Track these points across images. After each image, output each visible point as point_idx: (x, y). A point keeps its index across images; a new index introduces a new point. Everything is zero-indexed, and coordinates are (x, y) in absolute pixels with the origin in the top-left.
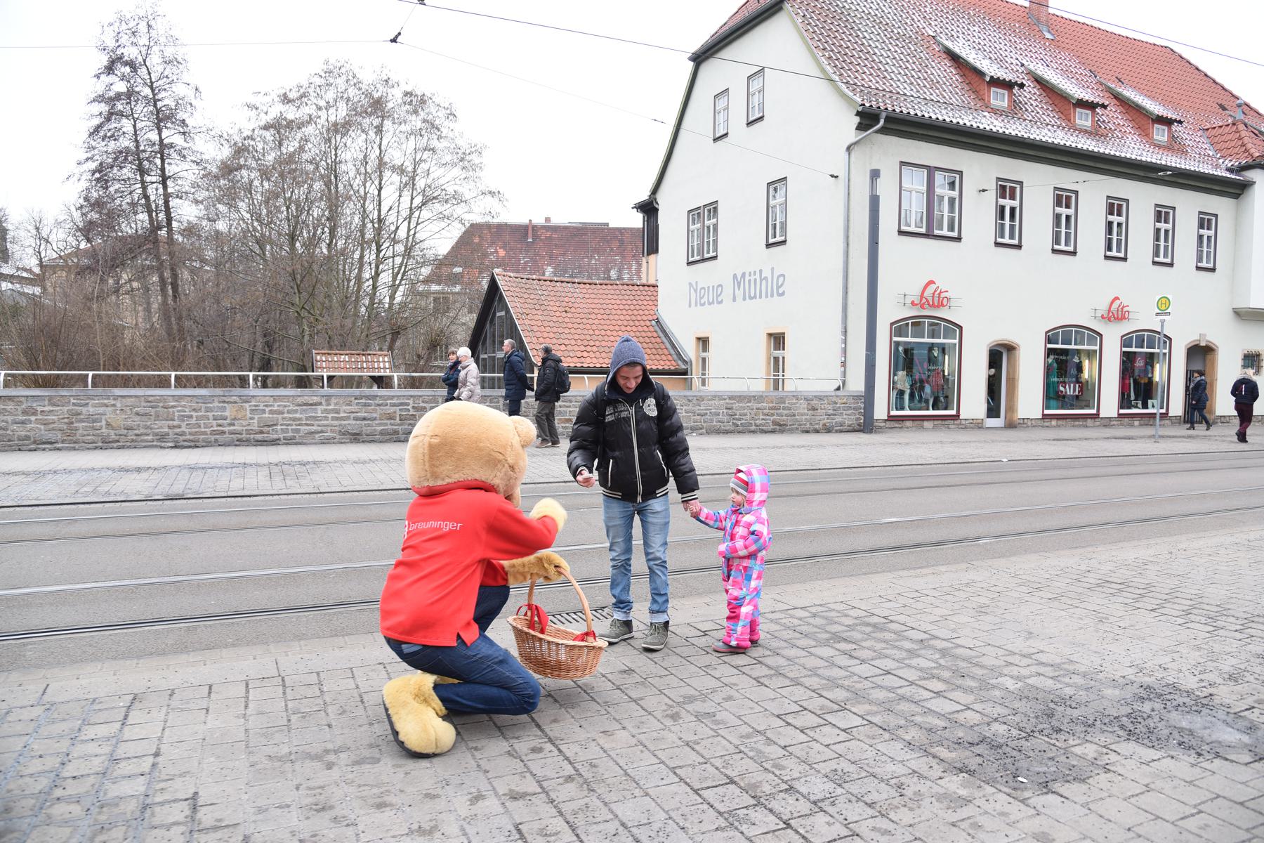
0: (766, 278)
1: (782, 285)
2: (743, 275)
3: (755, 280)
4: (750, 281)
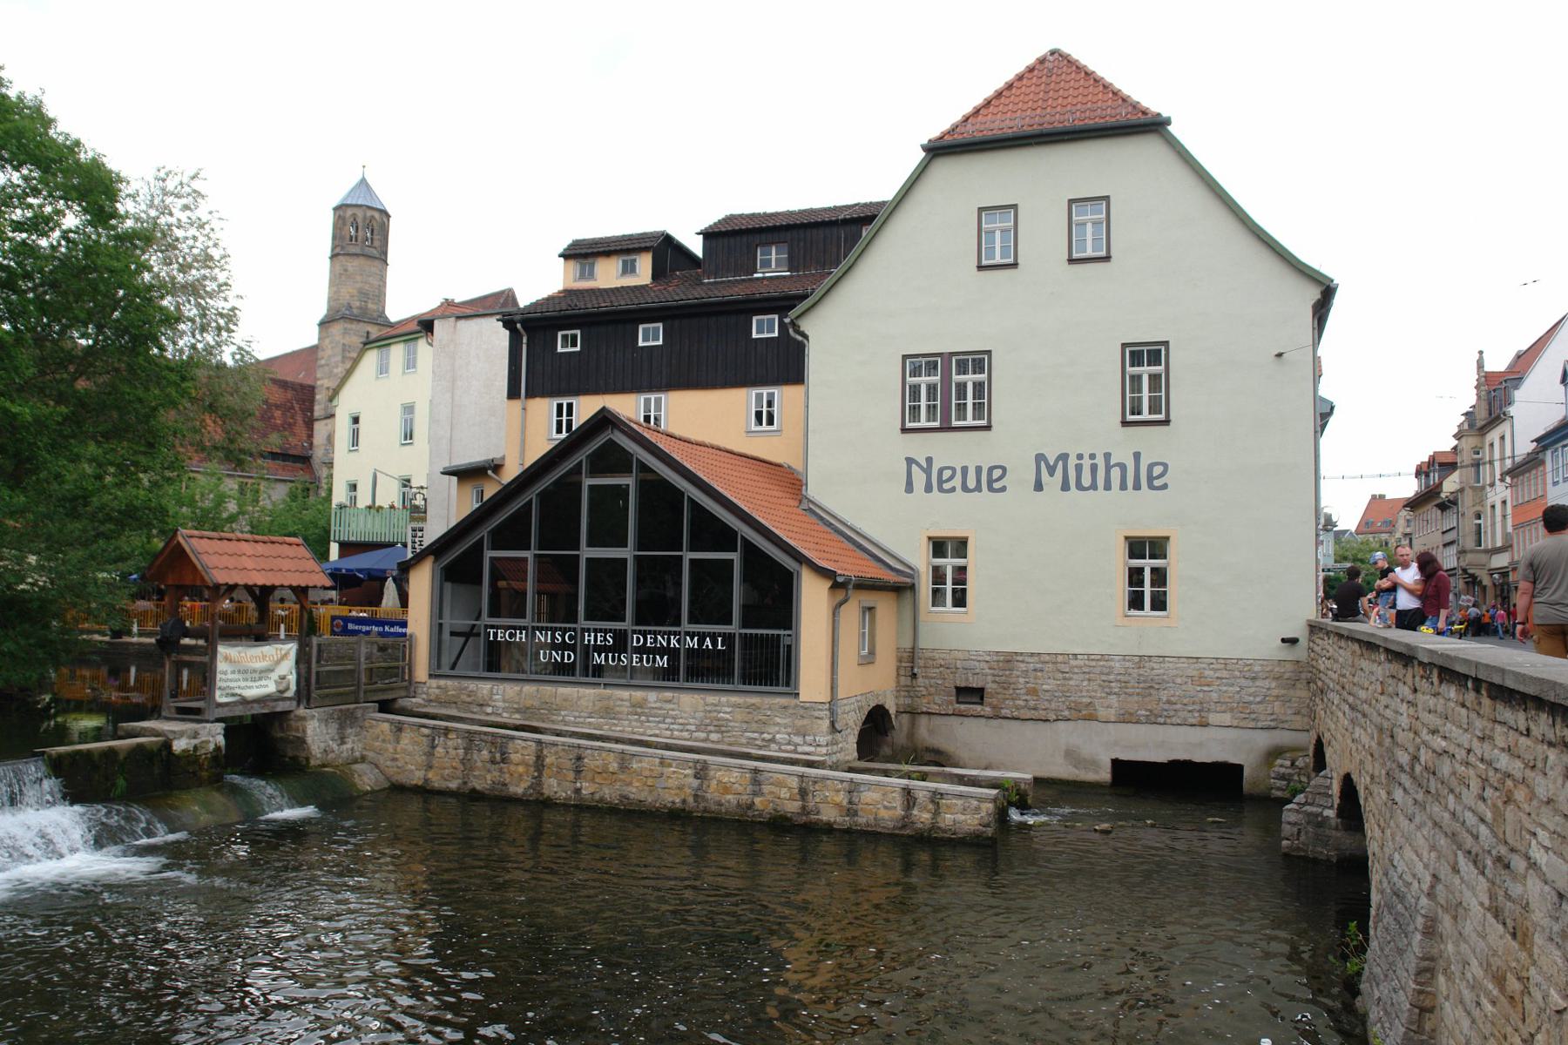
2: (1064, 457)
3: (1094, 468)
4: (1079, 468)
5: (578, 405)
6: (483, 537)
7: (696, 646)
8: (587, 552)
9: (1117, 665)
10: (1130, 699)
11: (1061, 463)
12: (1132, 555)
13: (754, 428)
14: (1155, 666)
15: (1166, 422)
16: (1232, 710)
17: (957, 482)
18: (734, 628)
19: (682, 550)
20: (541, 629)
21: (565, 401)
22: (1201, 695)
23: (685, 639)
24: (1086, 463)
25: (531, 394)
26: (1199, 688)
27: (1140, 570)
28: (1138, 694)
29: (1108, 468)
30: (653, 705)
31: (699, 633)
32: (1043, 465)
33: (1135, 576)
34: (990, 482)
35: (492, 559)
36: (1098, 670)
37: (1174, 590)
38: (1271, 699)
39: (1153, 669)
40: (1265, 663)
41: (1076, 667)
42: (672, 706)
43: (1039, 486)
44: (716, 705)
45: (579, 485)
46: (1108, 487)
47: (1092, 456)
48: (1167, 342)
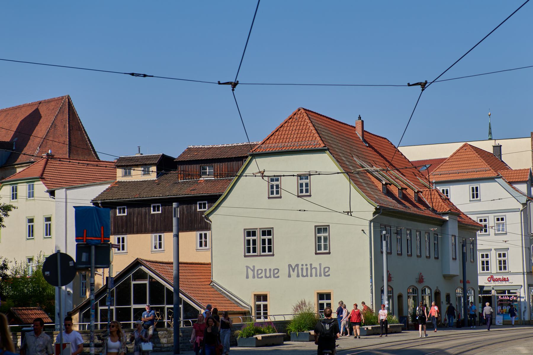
0: (316, 268)
1: (327, 272)
2: (297, 265)
3: (307, 269)
4: (302, 269)
8: (134, 306)
11: (296, 267)
13: (199, 248)
15: (329, 253)
17: (263, 274)
19: (164, 305)
21: (121, 237)
24: (304, 267)
27: (323, 304)
29: (311, 269)
32: (291, 268)
34: (274, 274)
35: (101, 310)
43: (290, 276)
45: (130, 284)
46: (311, 276)
47: (306, 265)
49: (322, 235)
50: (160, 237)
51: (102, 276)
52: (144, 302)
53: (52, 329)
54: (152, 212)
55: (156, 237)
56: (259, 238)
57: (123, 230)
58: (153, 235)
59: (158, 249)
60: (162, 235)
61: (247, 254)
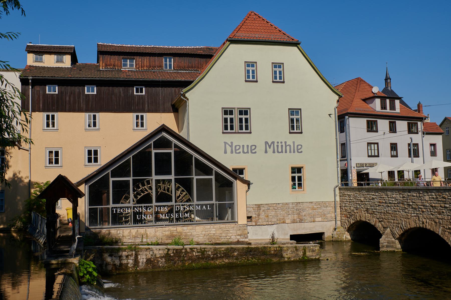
0: (290, 145)
1: (300, 149)
2: (273, 143)
3: (282, 146)
4: (278, 146)
5: (58, 116)
6: (109, 172)
7: (200, 209)
9: (291, 206)
10: (294, 216)
11: (272, 145)
12: (292, 173)
14: (301, 205)
15: (301, 133)
16: (321, 216)
17: (241, 150)
18: (214, 202)
20: (137, 207)
21: (50, 114)
22: (313, 213)
23: (196, 207)
24: (280, 144)
25: (33, 111)
26: (312, 211)
28: (297, 214)
30: (185, 231)
31: (200, 204)
32: (267, 145)
33: (293, 179)
35: (113, 181)
36: (285, 208)
37: (305, 182)
38: (331, 212)
39: (300, 206)
40: (329, 202)
41: (279, 207)
42: (193, 231)
43: (266, 152)
44: (209, 229)
45: (150, 152)
46: (286, 152)
47: (281, 143)
48: (301, 109)
49: (295, 117)
50: (95, 117)
51: (29, 152)
52: (170, 173)
53: (143, 205)
54: (86, 93)
55: (89, 116)
56: (236, 116)
57: (54, 108)
58: (87, 114)
59: (92, 128)
60: (97, 114)
61: (225, 131)
